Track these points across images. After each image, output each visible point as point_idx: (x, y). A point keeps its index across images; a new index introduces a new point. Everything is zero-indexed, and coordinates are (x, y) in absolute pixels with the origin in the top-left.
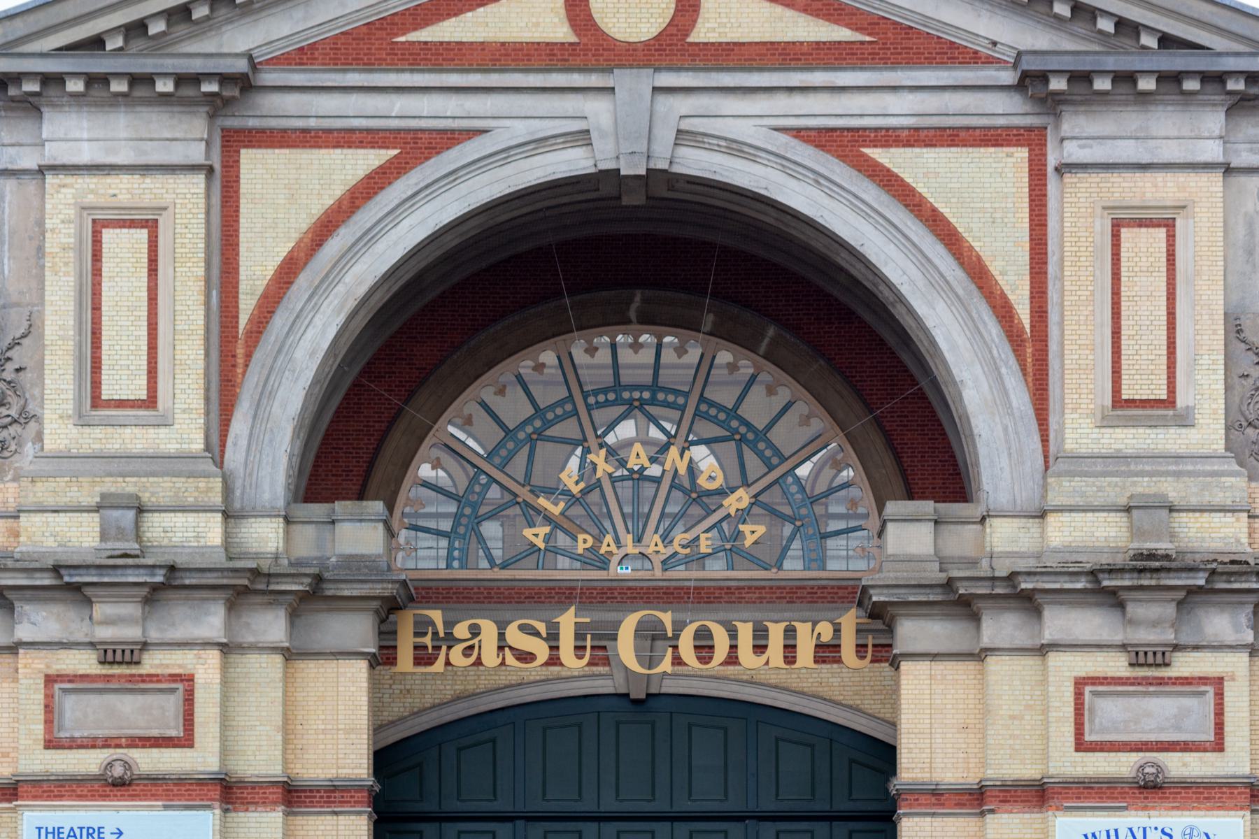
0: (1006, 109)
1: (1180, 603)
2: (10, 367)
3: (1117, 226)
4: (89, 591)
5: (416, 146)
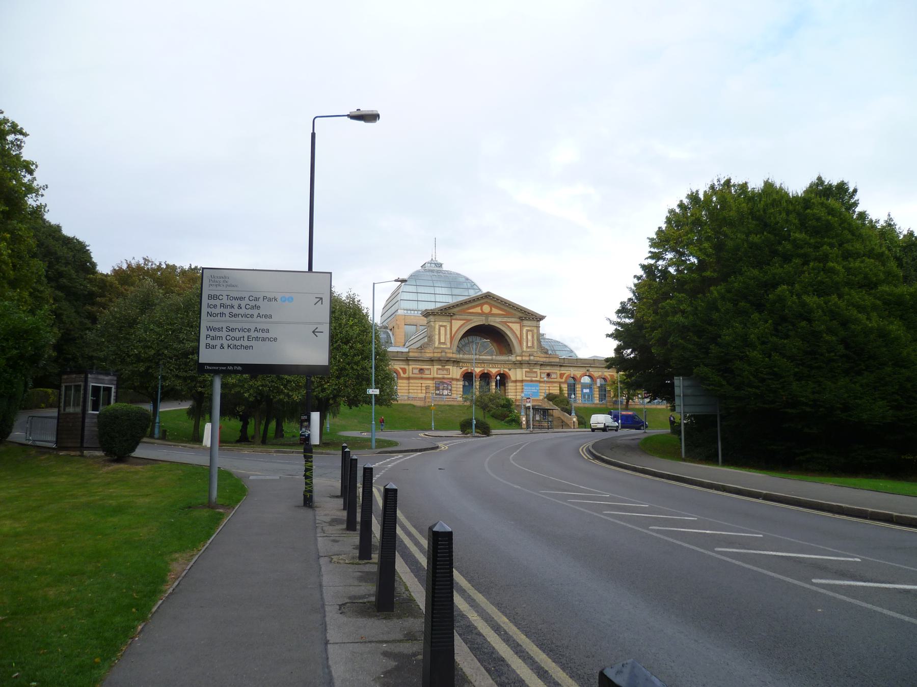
0: (518, 320)
5: (468, 320)
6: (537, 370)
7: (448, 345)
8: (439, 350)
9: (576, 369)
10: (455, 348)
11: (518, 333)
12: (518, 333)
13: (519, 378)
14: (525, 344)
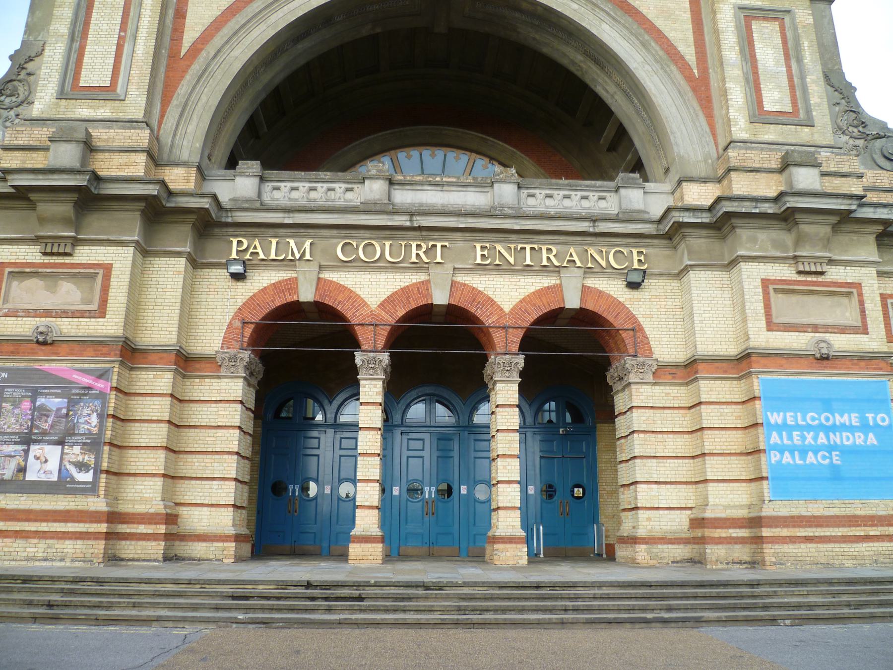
1: (835, 228)
2: (23, 73)
3: (748, 19)
4: (33, 196)
7: (135, 103)
8: (41, 134)
10: (190, 133)
13: (716, 340)
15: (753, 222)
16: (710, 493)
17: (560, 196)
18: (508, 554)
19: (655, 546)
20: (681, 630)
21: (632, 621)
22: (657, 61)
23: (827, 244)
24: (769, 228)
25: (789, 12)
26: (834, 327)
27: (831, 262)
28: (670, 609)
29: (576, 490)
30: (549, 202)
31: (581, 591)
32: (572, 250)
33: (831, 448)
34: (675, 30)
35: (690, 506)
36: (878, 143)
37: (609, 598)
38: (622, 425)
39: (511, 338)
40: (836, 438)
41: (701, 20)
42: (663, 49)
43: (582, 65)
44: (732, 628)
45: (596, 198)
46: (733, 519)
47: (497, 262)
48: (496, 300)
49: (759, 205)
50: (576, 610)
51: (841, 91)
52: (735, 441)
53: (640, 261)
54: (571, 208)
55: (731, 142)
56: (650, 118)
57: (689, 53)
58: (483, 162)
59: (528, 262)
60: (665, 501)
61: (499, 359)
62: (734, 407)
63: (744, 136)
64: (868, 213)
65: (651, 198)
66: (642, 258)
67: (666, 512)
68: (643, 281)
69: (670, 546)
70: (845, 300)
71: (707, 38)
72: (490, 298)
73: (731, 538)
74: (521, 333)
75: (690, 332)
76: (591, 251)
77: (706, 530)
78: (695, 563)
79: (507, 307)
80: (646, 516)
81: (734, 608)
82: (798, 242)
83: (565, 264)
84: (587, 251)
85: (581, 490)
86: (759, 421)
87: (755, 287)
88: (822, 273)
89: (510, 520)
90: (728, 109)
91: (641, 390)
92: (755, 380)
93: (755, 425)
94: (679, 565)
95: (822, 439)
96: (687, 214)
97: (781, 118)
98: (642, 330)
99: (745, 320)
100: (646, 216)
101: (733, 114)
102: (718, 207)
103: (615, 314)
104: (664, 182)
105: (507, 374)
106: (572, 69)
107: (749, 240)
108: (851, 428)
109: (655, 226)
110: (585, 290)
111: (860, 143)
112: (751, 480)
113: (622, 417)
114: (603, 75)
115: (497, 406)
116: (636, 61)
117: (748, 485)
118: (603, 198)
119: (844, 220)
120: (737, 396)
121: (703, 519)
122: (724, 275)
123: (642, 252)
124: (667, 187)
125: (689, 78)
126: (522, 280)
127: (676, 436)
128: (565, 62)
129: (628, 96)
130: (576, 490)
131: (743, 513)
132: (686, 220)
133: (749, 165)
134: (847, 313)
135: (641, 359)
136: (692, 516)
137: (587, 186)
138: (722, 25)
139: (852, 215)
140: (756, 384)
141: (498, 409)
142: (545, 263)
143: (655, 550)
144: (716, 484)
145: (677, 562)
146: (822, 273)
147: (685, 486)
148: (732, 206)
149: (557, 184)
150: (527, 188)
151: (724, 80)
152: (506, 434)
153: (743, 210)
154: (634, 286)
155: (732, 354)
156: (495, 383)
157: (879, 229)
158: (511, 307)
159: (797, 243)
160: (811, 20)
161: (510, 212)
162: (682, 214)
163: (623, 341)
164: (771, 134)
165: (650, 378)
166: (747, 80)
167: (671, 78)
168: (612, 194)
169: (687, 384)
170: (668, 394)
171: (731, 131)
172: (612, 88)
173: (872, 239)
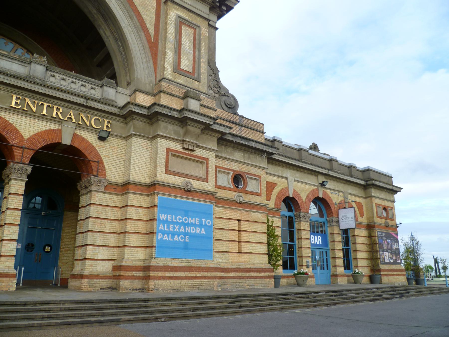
1: (202, 131)
6: (208, 151)
9: (298, 175)
11: (149, 18)
12: (149, 18)
13: (140, 174)
14: (170, 57)
15: (167, 119)
16: (126, 252)
17: (70, 81)
18: (3, 284)
19: (93, 280)
20: (110, 327)
21: (83, 323)
22: (135, 27)
23: (197, 137)
24: (174, 124)
25: (199, 27)
26: (194, 176)
27: (198, 146)
28: (103, 315)
29: (47, 247)
30: (62, 82)
31: (52, 306)
32: (71, 112)
33: (185, 234)
34: (147, 15)
35: (113, 259)
36: (224, 98)
37: (69, 310)
38: (82, 213)
39: (25, 154)
40: (188, 229)
41: (160, 15)
42: (139, 22)
43: (95, 15)
44: (136, 324)
45: (90, 87)
46: (136, 266)
47: (25, 109)
48: (20, 130)
49: (172, 112)
50: (49, 318)
51: (214, 71)
52: (141, 227)
53: (107, 126)
54: (75, 89)
55: (163, 78)
56: (126, 55)
57: (151, 29)
58: (22, 51)
59: (44, 113)
60: (101, 256)
61: (15, 166)
62: (143, 209)
63: (170, 77)
64: (216, 127)
65: (119, 96)
66: (109, 125)
67: (101, 262)
68: (107, 137)
69: (101, 280)
70: (201, 165)
71: (161, 25)
72: (16, 129)
73: (133, 276)
74: (32, 153)
75: (128, 168)
76: (82, 115)
77: (122, 272)
78: (113, 289)
79: (26, 136)
80: (89, 263)
81: (137, 313)
82: (186, 133)
83: (66, 119)
84: (80, 114)
85: (50, 247)
86: (155, 218)
87: (163, 152)
88: (193, 151)
89: (7, 263)
90: (164, 62)
91: (97, 195)
92: (156, 197)
93: (153, 219)
94: (104, 290)
95: (182, 229)
96: (137, 108)
97: (187, 74)
98: (102, 163)
99: (155, 167)
100: (115, 104)
101: (166, 65)
102: (152, 108)
103: (89, 152)
104: (126, 89)
105: (20, 175)
106: (89, 16)
107: (165, 127)
108: (195, 225)
109: (119, 110)
110: (75, 136)
111: (217, 96)
112: (147, 247)
113: (83, 209)
114: (105, 25)
115: (10, 194)
116: (124, 23)
117: (145, 249)
118: (94, 89)
119: (206, 128)
120: (146, 204)
121: (121, 266)
122: (149, 143)
123: (109, 122)
124: (128, 92)
125: (149, 41)
126: (39, 123)
127: (111, 222)
128: (86, 11)
129: (116, 40)
130: (47, 247)
131: (140, 264)
132: (136, 111)
133: (170, 92)
134: (199, 171)
135: (99, 178)
136: (114, 264)
137: (86, 80)
138: (169, 21)
139: (210, 127)
140: (156, 199)
141: (10, 196)
142: (54, 115)
143: (92, 282)
144: (129, 248)
145: (104, 289)
146: (193, 151)
147: (112, 248)
148: (160, 109)
149: (69, 74)
150: (51, 71)
151: (165, 48)
152: (13, 211)
153: (164, 112)
154: (102, 139)
155: (147, 182)
156: (11, 179)
157: (219, 135)
158: (29, 136)
159: (186, 134)
160: (207, 35)
161: (39, 81)
162: (134, 107)
163: (91, 167)
164: (181, 80)
165: (103, 189)
166: (175, 51)
167: (140, 38)
168: (99, 88)
169: (121, 195)
170: (110, 199)
171: (164, 73)
172: (108, 33)
173: (216, 139)
